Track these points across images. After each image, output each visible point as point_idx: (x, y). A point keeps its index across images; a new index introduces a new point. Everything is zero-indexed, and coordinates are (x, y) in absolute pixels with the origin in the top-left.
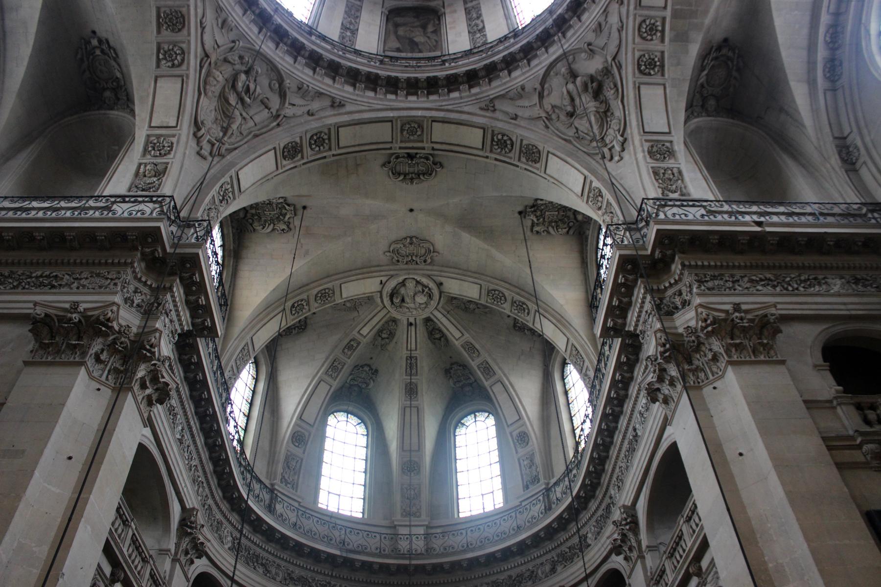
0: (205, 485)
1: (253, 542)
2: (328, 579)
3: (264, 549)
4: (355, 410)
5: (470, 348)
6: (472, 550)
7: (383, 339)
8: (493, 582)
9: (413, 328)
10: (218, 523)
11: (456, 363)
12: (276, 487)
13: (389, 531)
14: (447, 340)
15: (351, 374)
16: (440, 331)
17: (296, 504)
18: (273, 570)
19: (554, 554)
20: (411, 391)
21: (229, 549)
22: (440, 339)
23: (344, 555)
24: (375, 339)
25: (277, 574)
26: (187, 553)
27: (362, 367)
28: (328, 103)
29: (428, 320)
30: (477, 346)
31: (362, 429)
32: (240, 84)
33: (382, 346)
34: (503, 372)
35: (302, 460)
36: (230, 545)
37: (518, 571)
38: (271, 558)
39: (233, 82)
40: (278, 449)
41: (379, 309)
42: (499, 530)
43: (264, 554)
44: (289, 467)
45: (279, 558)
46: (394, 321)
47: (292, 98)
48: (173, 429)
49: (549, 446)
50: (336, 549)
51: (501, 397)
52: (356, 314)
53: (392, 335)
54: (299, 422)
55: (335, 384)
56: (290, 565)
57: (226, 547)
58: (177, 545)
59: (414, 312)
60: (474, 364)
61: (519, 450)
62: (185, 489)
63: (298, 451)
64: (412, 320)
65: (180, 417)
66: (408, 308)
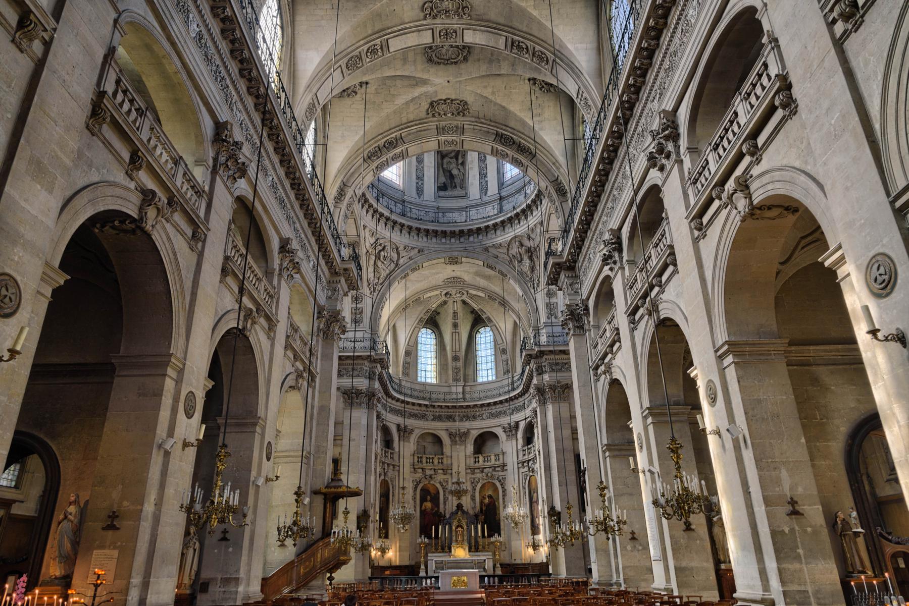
5: (482, 311)
20: (455, 326)
28: (416, 250)
31: (433, 336)
32: (382, 257)
39: (378, 257)
47: (402, 253)
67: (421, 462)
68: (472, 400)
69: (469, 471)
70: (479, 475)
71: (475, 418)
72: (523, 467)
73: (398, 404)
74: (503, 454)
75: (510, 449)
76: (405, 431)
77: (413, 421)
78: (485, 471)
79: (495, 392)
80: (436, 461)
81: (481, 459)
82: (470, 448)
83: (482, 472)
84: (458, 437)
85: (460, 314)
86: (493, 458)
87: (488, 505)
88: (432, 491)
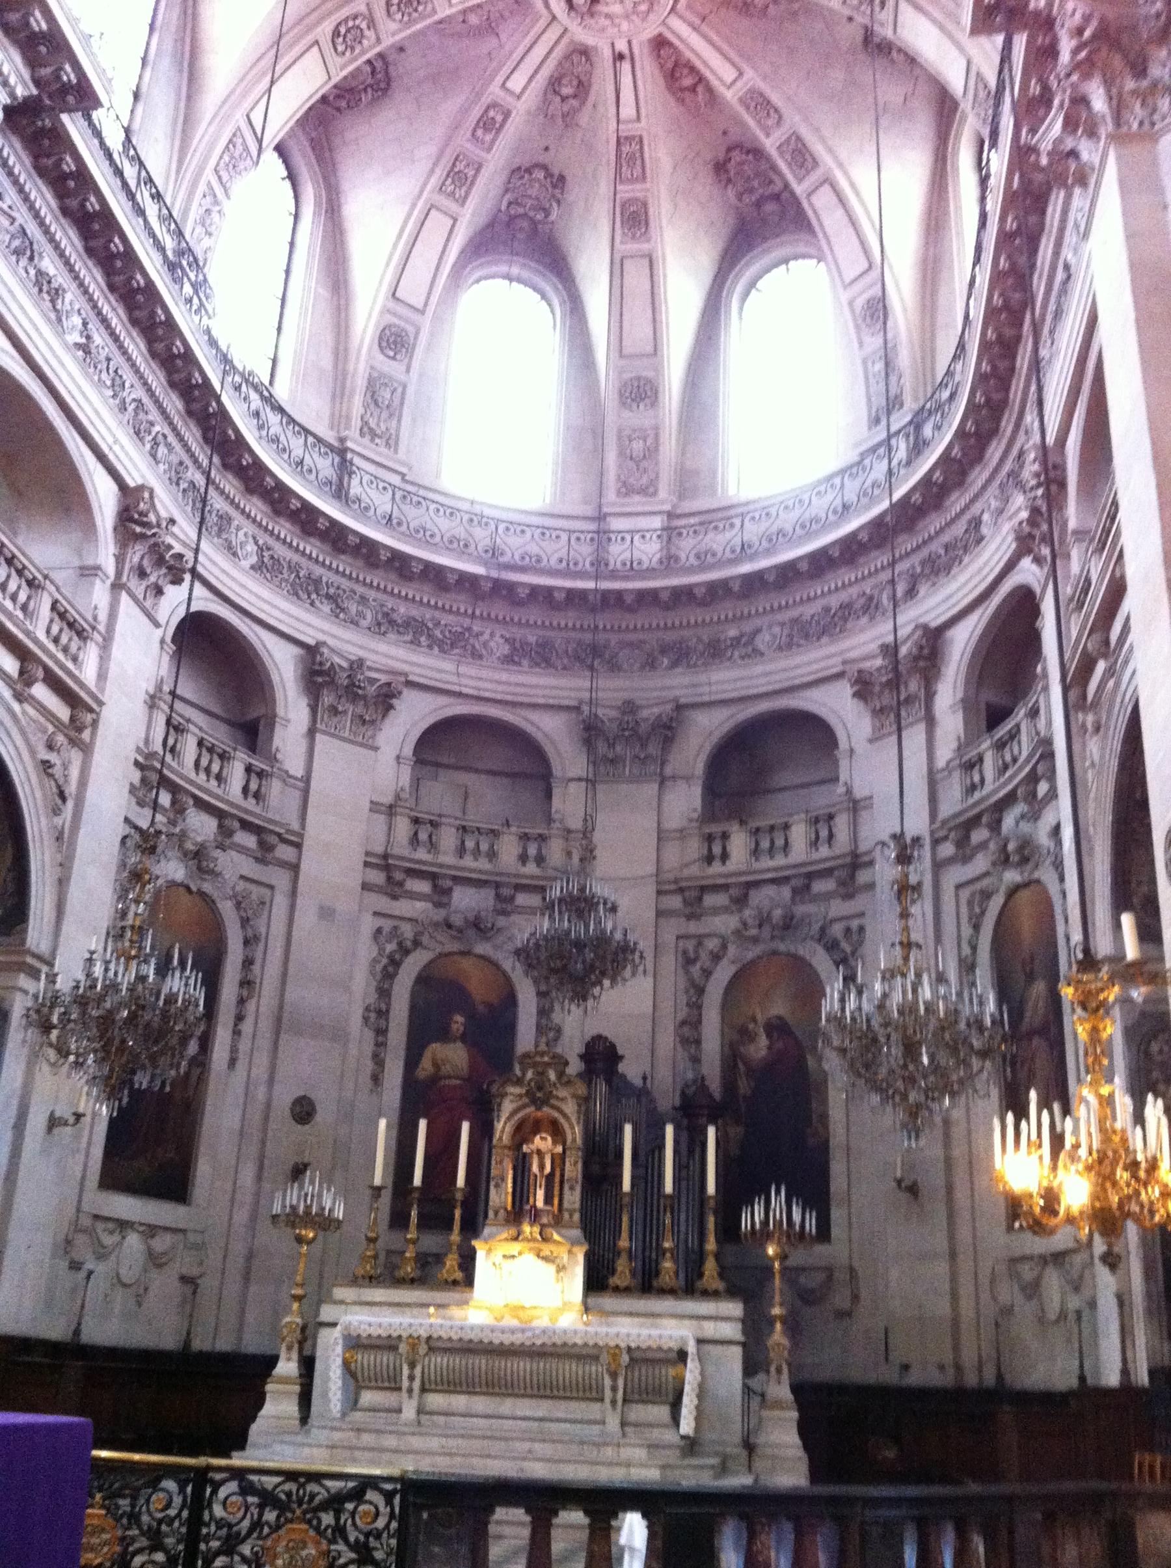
0: (171, 438)
1: (303, 553)
2: (467, 622)
3: (330, 568)
4: (525, 274)
5: (759, 103)
6: (752, 558)
7: (564, 99)
8: (795, 621)
9: (626, 66)
10: (221, 517)
11: (738, 146)
12: (349, 444)
13: (593, 526)
14: (710, 90)
15: (507, 191)
16: (693, 69)
17: (396, 480)
18: (353, 608)
19: (916, 559)
21: (252, 567)
22: (693, 89)
23: (494, 574)
24: (546, 102)
25: (360, 614)
26: (142, 574)
27: (529, 171)
29: (660, 43)
30: (775, 98)
33: (564, 116)
34: (836, 158)
35: (405, 387)
36: (254, 559)
37: (843, 596)
38: (345, 584)
40: (351, 367)
41: (542, 24)
42: (807, 516)
43: (327, 576)
44: (376, 403)
45: (364, 583)
46: (585, 52)
48: (58, 320)
49: (933, 325)
50: (480, 564)
51: (829, 218)
52: (492, 42)
53: (583, 88)
54: (391, 304)
55: (472, 214)
56: (384, 597)
57: (246, 564)
58: (120, 559)
59: (625, 26)
60: (770, 144)
61: (868, 340)
62: (116, 448)
63: (394, 369)
64: (621, 46)
65: (71, 297)
66: (607, 16)
67: (432, 846)
68: (704, 560)
69: (675, 902)
70: (725, 923)
71: (716, 652)
72: (965, 852)
73: (312, 547)
74: (856, 806)
75: (893, 779)
76: (352, 691)
77: (401, 652)
78: (761, 898)
79: (820, 506)
80: (509, 849)
81: (739, 844)
82: (685, 801)
83: (741, 901)
84: (627, 744)
85: (662, 155)
86: (799, 834)
87: (766, 1072)
88: (478, 987)
